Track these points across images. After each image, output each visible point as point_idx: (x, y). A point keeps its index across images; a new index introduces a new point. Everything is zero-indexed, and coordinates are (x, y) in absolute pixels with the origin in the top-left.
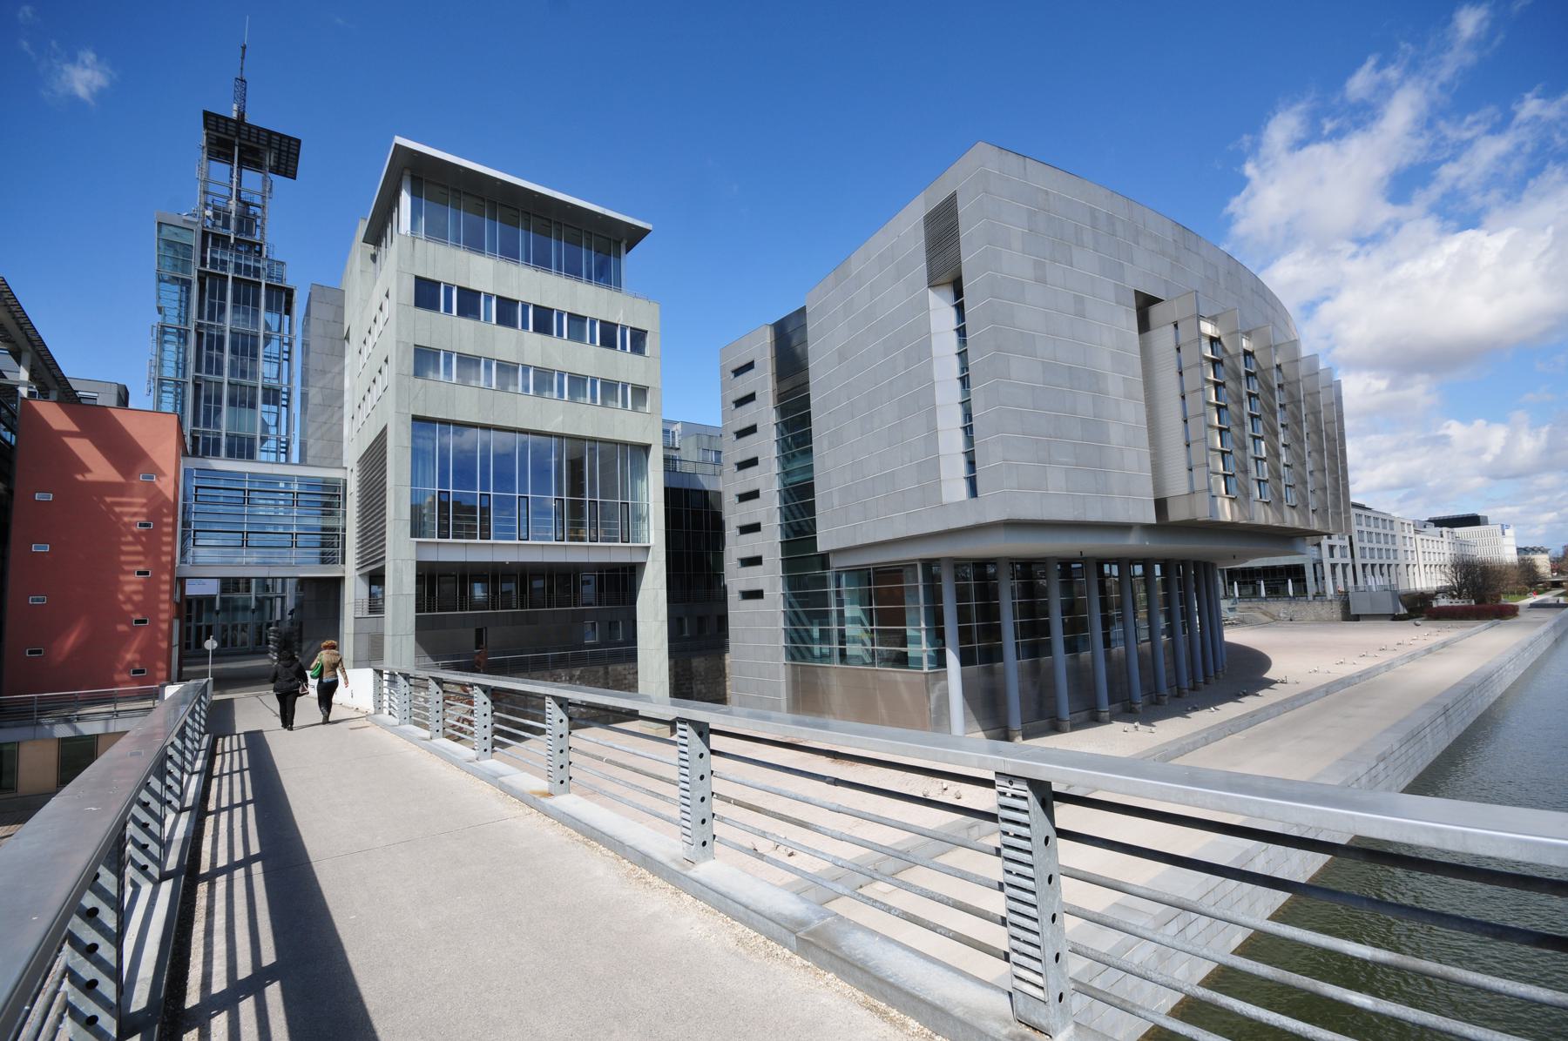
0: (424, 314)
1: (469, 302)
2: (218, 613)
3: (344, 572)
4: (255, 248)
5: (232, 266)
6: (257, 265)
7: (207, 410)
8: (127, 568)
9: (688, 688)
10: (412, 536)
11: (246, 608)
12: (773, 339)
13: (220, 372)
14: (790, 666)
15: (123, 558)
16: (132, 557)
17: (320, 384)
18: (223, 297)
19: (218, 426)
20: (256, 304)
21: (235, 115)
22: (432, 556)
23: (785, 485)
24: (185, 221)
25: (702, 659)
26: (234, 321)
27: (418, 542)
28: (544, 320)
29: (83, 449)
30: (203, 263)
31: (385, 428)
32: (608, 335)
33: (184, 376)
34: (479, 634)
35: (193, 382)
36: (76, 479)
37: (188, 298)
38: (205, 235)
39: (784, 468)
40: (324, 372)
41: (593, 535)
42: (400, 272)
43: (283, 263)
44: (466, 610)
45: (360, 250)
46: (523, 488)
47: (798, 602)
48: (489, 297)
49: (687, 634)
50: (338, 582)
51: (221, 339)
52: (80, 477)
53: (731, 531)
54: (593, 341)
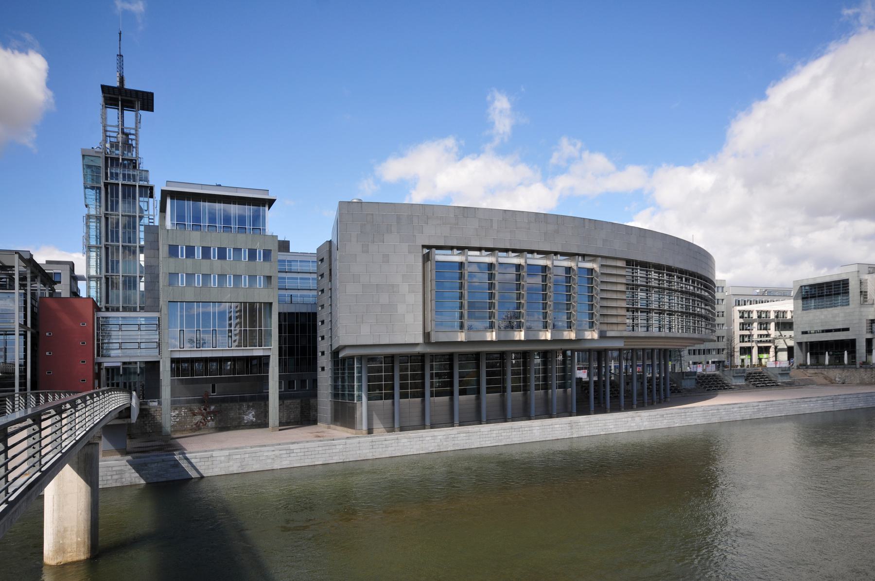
4: (134, 164)
9: (308, 413)
11: (135, 373)
14: (333, 402)
18: (117, 196)
19: (118, 272)
34: (213, 387)
35: (105, 246)
37: (100, 198)
43: (147, 171)
46: (214, 326)
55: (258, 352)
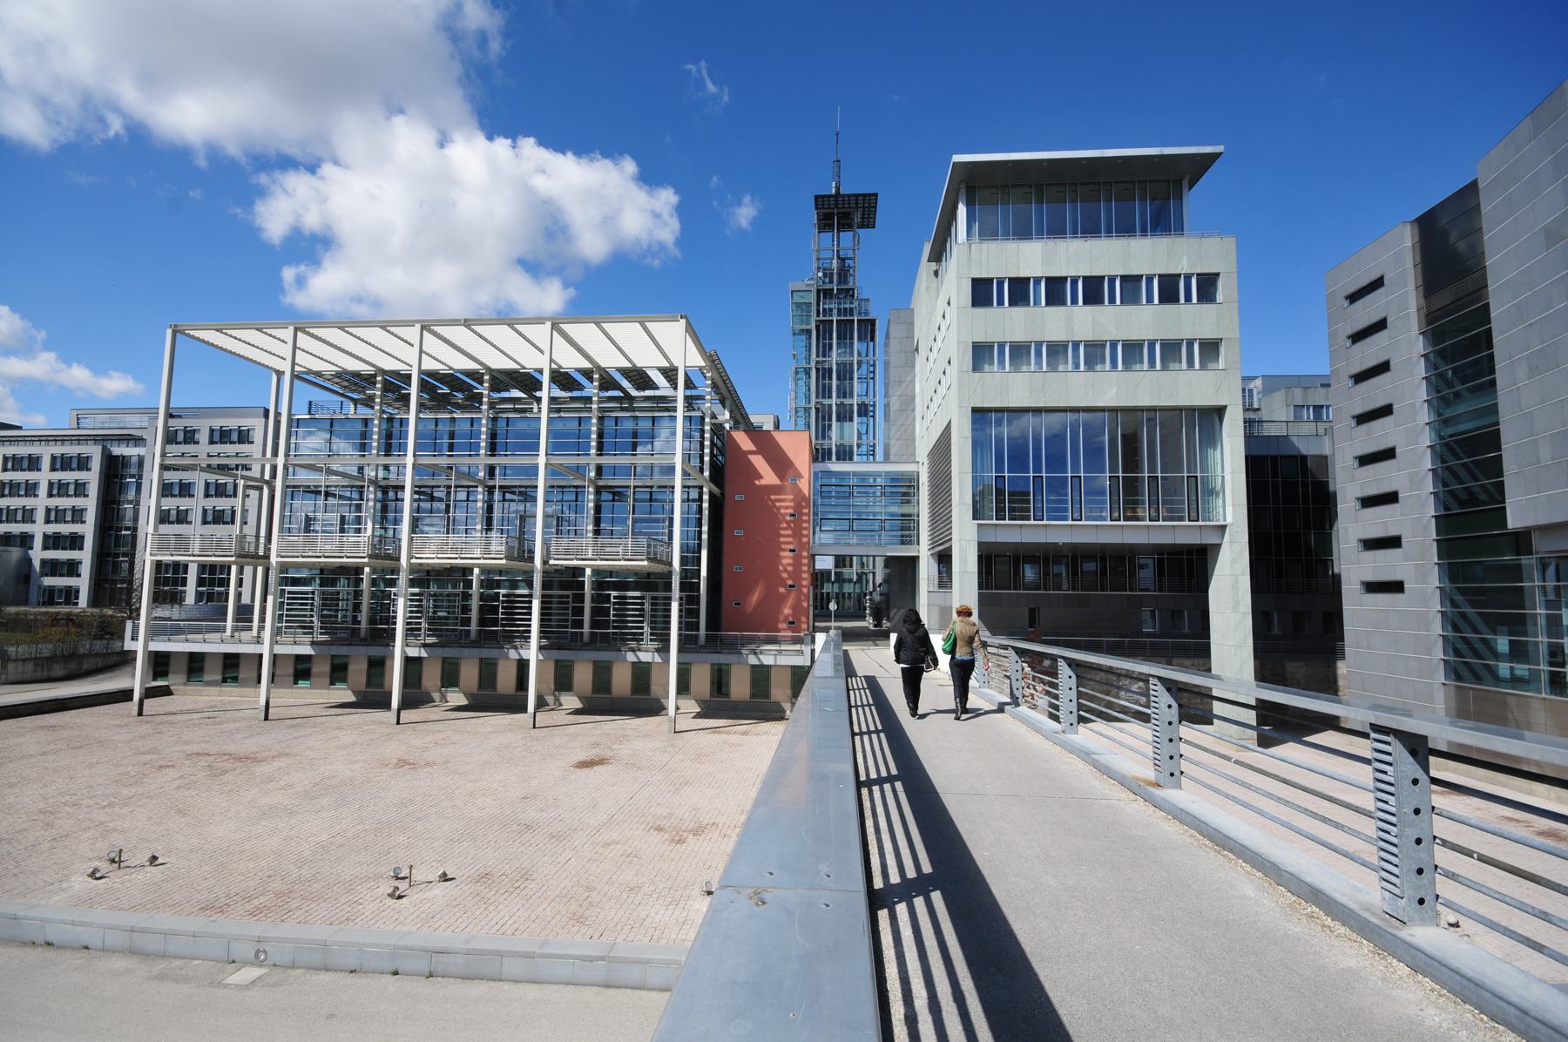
0: (980, 311)
1: (1019, 291)
2: (833, 583)
3: (919, 551)
4: (848, 293)
5: (835, 311)
6: (851, 306)
7: (824, 426)
8: (783, 546)
10: (974, 519)
12: (1417, 239)
13: (830, 397)
14: (1453, 689)
15: (782, 539)
16: (786, 539)
17: (898, 393)
18: (831, 338)
19: (830, 438)
20: (852, 338)
21: (834, 191)
22: (991, 537)
23: (1441, 438)
24: (807, 285)
25: (1302, 664)
26: (838, 355)
27: (978, 524)
28: (1094, 291)
29: (759, 462)
30: (818, 315)
31: (950, 422)
32: (1169, 290)
33: (809, 403)
36: (756, 485)
37: (810, 343)
38: (819, 291)
39: (1439, 415)
40: (901, 382)
41: (1153, 514)
42: (959, 278)
43: (868, 300)
44: (1020, 589)
45: (926, 268)
46: (1075, 468)
47: (1467, 600)
48: (1037, 281)
49: (1276, 631)
50: (913, 561)
51: (830, 370)
52: (757, 482)
53: (1346, 505)
54: (1150, 300)
55: (1180, 532)
